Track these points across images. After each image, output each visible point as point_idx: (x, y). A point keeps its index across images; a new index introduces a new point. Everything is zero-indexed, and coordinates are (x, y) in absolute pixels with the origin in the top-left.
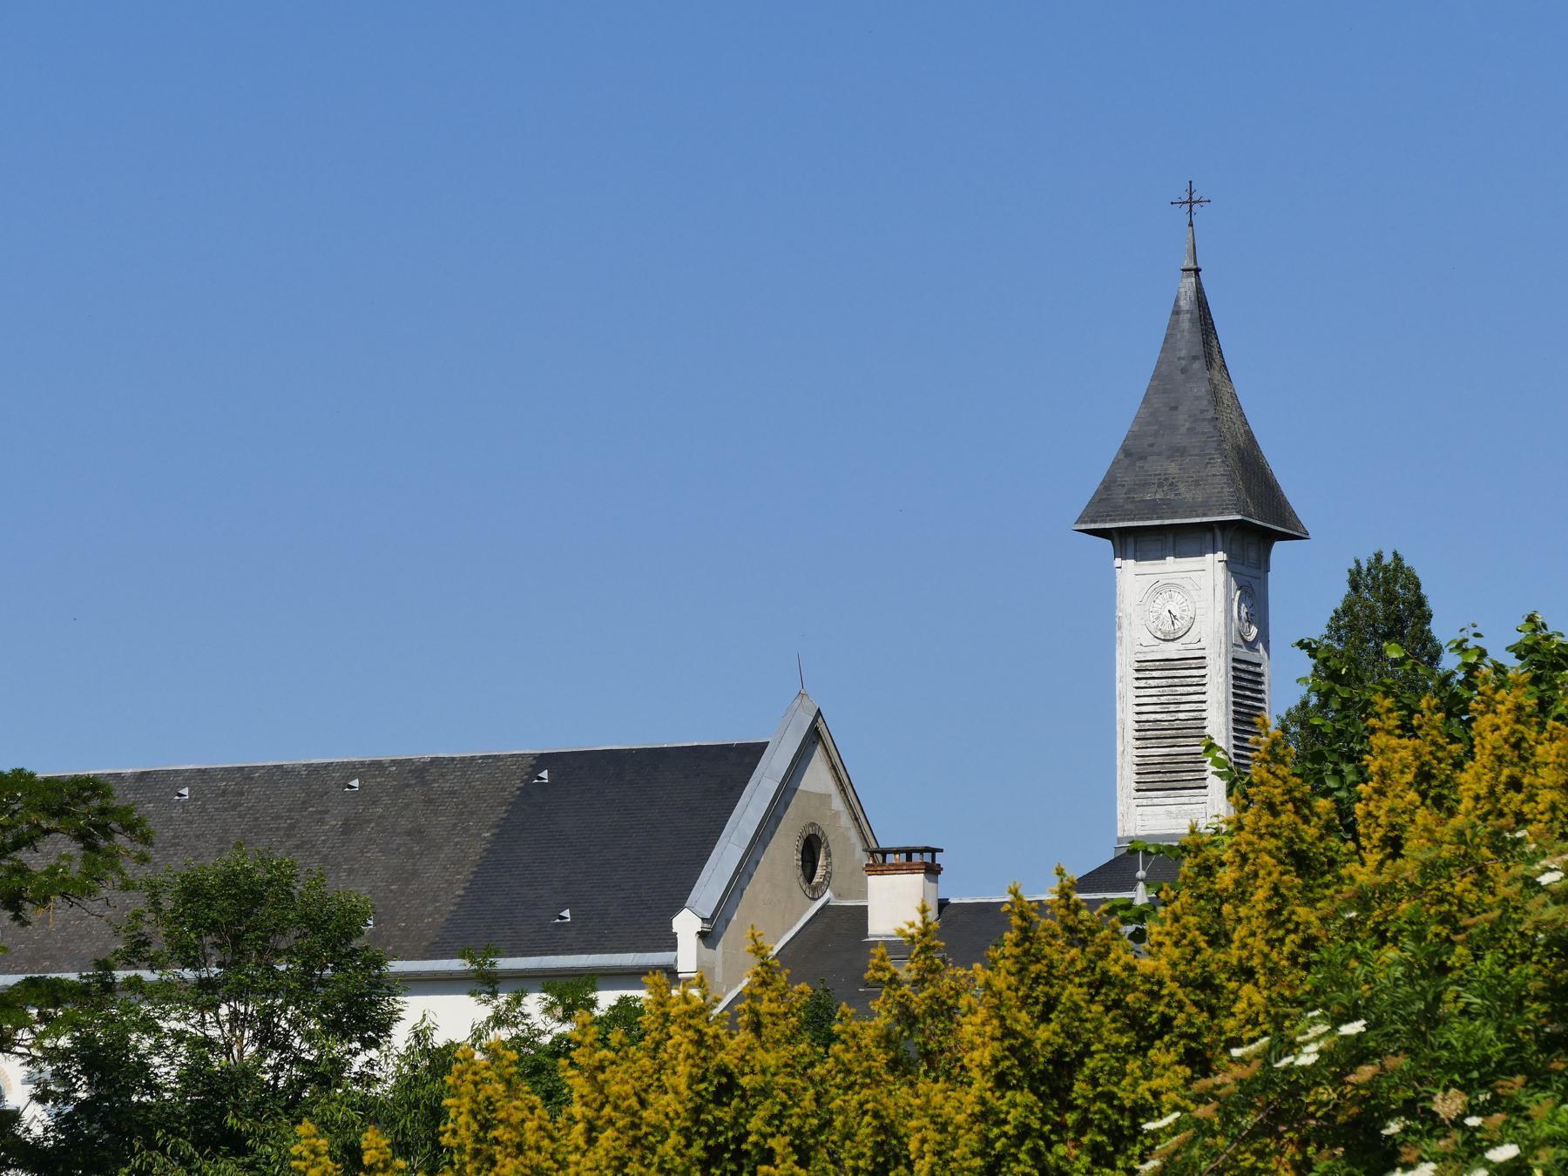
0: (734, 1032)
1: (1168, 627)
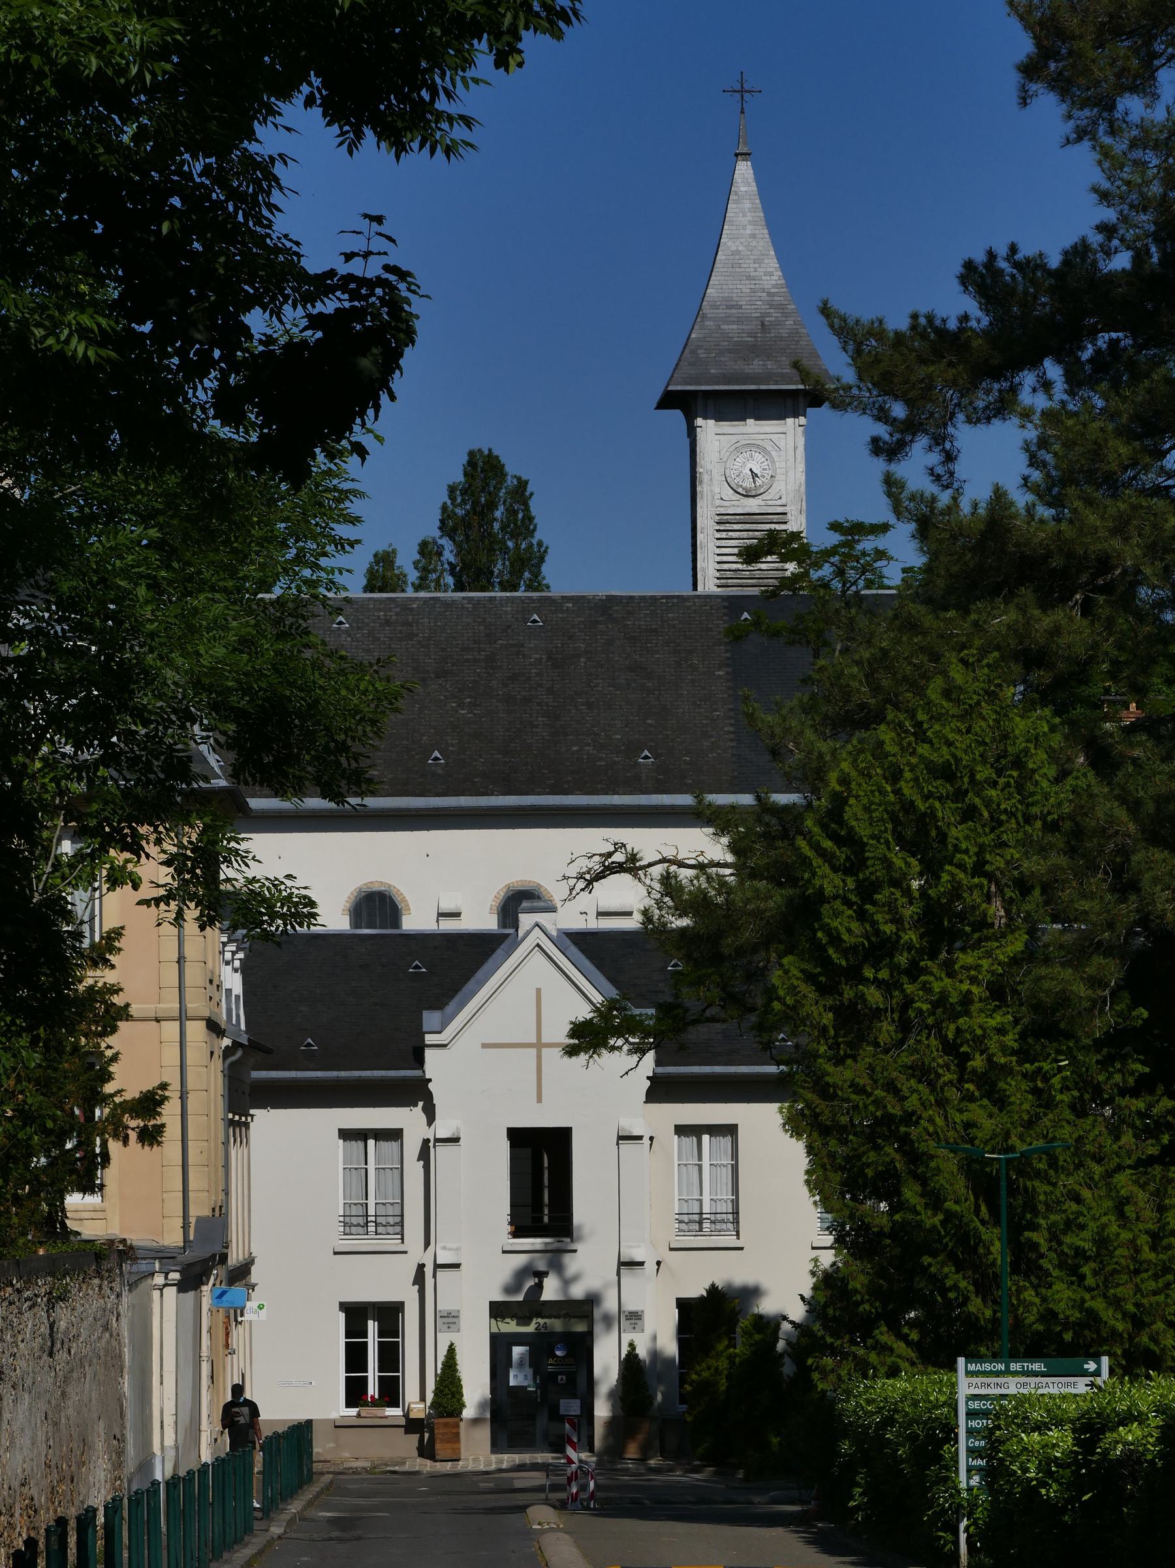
0: (983, 1047)
1: (749, 483)
